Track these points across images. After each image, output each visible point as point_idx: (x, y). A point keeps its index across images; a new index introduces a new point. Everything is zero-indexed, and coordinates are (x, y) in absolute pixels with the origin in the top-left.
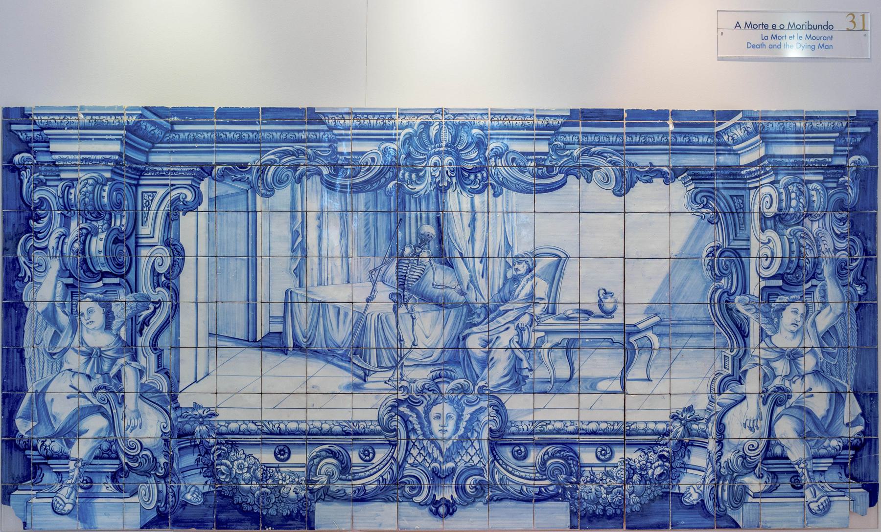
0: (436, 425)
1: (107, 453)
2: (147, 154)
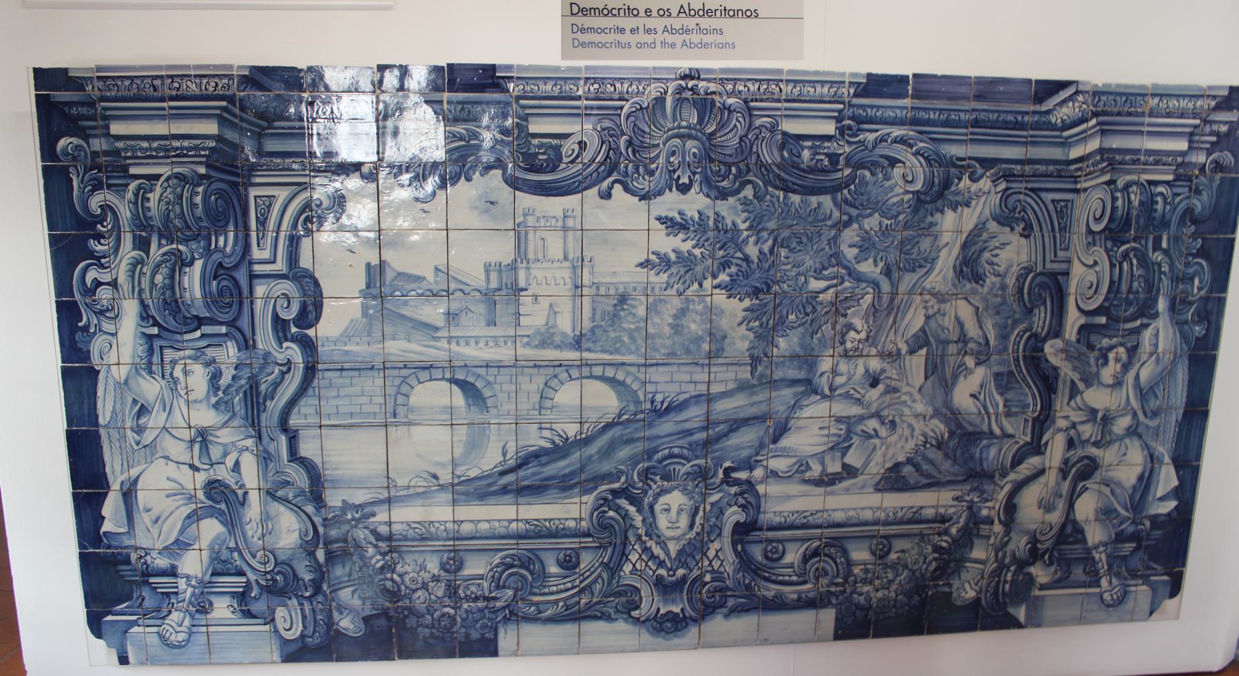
0: (662, 522)
1: (220, 567)
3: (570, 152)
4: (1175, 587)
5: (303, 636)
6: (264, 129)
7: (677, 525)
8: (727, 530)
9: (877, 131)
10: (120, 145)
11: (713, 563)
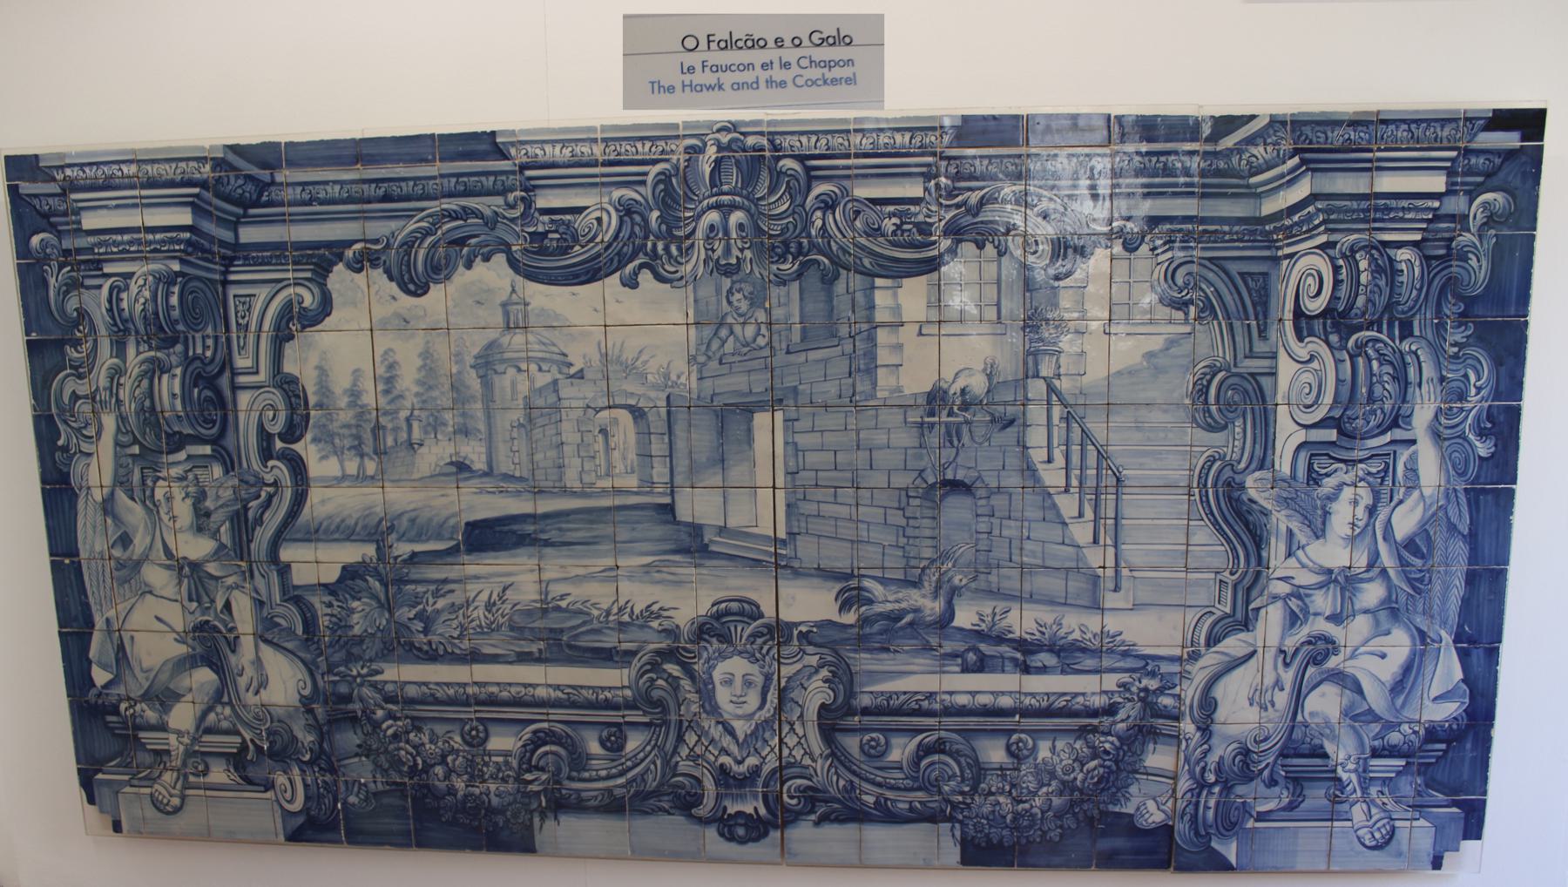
0: (723, 696)
2: (234, 226)
4: (1473, 824)
5: (305, 810)
6: (238, 217)
8: (812, 712)
9: (981, 188)
11: (794, 753)
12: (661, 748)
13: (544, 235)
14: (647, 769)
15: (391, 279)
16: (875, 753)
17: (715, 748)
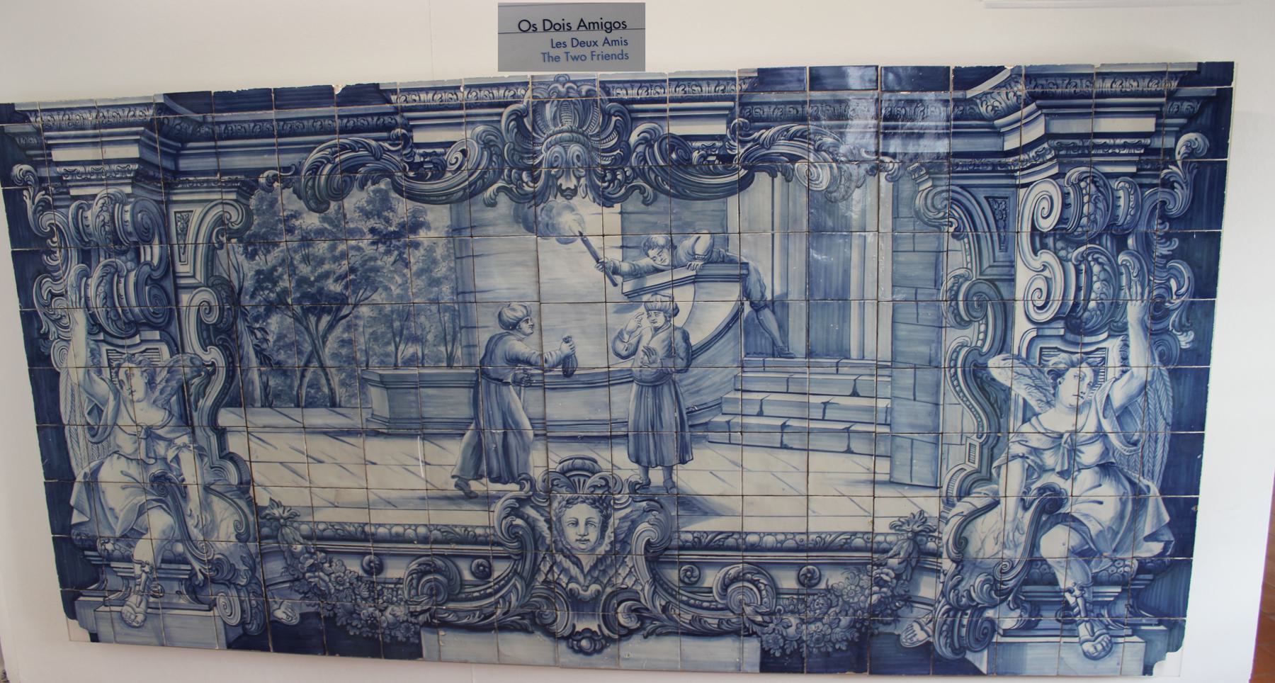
0: (572, 534)
2: (176, 157)
3: (454, 161)
5: (243, 623)
6: (179, 149)
7: (586, 538)
10: (61, 169)
12: (522, 577)
13: (421, 164)
14: (509, 592)
15: (300, 198)
16: (691, 584)
17: (566, 576)
